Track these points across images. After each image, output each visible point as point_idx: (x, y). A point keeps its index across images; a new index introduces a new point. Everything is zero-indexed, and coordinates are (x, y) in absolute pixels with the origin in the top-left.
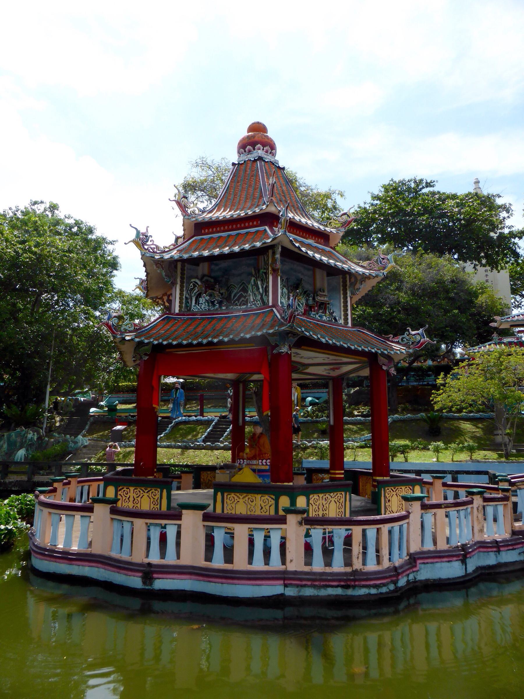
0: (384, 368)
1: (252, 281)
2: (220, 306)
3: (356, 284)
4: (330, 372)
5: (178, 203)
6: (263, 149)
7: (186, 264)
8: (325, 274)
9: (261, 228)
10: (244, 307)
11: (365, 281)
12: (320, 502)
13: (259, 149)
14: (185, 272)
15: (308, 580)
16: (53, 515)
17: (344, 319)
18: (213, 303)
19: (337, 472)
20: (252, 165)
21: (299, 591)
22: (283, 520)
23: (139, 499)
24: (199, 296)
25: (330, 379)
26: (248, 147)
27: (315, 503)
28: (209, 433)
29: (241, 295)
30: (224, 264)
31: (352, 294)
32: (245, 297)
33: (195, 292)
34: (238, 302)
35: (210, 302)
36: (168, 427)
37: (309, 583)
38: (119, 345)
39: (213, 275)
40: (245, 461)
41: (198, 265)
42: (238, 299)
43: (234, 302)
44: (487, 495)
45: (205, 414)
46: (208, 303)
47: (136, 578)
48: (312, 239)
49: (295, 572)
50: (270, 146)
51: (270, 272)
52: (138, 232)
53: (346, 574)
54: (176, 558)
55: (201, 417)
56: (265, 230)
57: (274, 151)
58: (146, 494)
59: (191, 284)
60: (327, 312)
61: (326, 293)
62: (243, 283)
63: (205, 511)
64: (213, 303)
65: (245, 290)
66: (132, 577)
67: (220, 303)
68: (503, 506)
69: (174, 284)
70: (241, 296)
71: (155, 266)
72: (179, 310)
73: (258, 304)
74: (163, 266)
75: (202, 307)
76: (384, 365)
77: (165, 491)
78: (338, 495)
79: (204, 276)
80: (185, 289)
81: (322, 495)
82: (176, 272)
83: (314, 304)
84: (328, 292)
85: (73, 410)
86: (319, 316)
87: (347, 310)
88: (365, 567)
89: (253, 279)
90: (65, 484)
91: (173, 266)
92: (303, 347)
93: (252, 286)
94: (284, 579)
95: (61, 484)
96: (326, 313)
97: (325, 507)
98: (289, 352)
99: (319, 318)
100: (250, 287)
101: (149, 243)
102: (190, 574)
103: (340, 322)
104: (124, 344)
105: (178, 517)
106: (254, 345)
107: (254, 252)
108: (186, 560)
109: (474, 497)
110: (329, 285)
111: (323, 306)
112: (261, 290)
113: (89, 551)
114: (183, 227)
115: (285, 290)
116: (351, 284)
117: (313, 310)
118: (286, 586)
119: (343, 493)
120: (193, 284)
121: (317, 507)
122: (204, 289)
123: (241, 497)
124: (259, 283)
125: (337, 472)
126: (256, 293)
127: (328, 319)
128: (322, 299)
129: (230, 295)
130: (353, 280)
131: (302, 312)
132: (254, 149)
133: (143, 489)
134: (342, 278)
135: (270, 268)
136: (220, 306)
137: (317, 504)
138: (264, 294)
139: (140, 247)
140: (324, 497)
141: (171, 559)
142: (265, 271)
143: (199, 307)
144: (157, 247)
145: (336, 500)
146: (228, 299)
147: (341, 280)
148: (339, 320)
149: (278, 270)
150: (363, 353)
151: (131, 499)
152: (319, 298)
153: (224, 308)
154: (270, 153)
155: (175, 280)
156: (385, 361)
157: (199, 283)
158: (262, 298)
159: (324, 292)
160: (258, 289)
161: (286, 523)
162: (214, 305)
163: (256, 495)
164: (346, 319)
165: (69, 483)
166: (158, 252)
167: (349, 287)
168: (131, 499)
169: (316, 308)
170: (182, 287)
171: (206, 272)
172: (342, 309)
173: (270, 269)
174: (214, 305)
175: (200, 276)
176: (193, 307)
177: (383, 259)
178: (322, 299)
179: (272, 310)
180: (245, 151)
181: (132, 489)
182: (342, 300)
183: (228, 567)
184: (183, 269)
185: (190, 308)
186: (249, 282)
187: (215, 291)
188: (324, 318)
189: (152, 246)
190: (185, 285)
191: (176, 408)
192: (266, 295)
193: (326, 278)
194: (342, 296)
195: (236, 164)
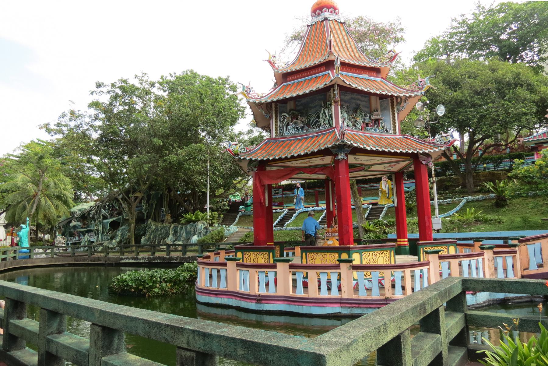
0: (424, 162)
1: (322, 111)
2: (302, 130)
3: (401, 103)
4: (390, 168)
5: (270, 62)
6: (328, 11)
8: (378, 98)
9: (326, 72)
10: (317, 129)
11: (408, 100)
12: (371, 257)
13: (325, 11)
15: (356, 304)
16: (205, 269)
17: (393, 130)
19: (402, 240)
20: (321, 24)
21: (351, 311)
22: (338, 267)
23: (256, 259)
24: (288, 124)
25: (393, 173)
26: (318, 11)
29: (317, 121)
30: (304, 101)
32: (319, 122)
36: (293, 216)
37: (357, 306)
38: (237, 162)
39: (298, 108)
41: (287, 103)
42: (315, 124)
44: (496, 250)
45: (320, 205)
46: (294, 129)
47: (252, 304)
48: (366, 74)
49: (348, 299)
50: (332, 8)
52: (244, 87)
53: (381, 300)
54: (275, 291)
55: (317, 208)
56: (329, 73)
57: (337, 11)
58: (260, 256)
59: (282, 117)
60: (380, 126)
61: (379, 112)
63: (291, 263)
64: (297, 128)
65: (319, 117)
66: (250, 303)
67: (302, 128)
68: (511, 258)
69: (271, 118)
70: (317, 121)
71: (257, 107)
75: (291, 132)
77: (271, 253)
78: (385, 252)
79: (291, 110)
80: (278, 121)
81: (372, 252)
82: (272, 110)
83: (370, 121)
84: (381, 111)
85: (228, 208)
86: (374, 130)
87: (395, 123)
88: (394, 296)
89: (323, 109)
90: (215, 254)
91: (269, 106)
92: (357, 154)
93: (323, 114)
94: (341, 303)
95: (213, 253)
96: (379, 127)
97: (375, 260)
98: (346, 158)
100: (321, 115)
101: (251, 92)
102: (284, 300)
104: (241, 162)
105: (274, 267)
107: (319, 92)
108: (281, 292)
109: (485, 251)
110: (381, 106)
111: (376, 122)
112: (328, 117)
113: (226, 290)
115: (345, 115)
116: (397, 103)
118: (341, 307)
119: (388, 251)
121: (368, 260)
122: (291, 119)
123: (318, 255)
124: (326, 111)
125: (402, 240)
126: (326, 119)
128: (376, 117)
129: (309, 122)
130: (399, 100)
132: (322, 12)
133: (258, 253)
134: (391, 100)
136: (302, 130)
139: (246, 96)
140: (374, 254)
141: (272, 292)
144: (257, 95)
145: (383, 256)
146: (308, 125)
147: (390, 101)
148: (390, 131)
149: (338, 101)
150: (407, 154)
151: (252, 259)
152: (374, 117)
153: (305, 131)
154: (334, 13)
155: (272, 115)
156: (424, 157)
157: (287, 116)
158: (329, 122)
159: (377, 111)
160: (326, 116)
162: (298, 130)
163: (326, 254)
164: (395, 130)
165: (219, 254)
167: (396, 106)
168: (252, 259)
169: (372, 124)
170: (276, 119)
171: (293, 107)
172: (392, 122)
173: (332, 102)
174: (298, 130)
175: (288, 112)
177: (421, 82)
178: (376, 117)
179: (334, 131)
180: (316, 15)
181: (252, 253)
182: (391, 116)
183: (306, 296)
184: (276, 108)
186: (321, 111)
188: (378, 131)
189: (254, 94)
190: (278, 118)
191: (298, 202)
193: (379, 101)
194: (391, 113)
195: (309, 26)
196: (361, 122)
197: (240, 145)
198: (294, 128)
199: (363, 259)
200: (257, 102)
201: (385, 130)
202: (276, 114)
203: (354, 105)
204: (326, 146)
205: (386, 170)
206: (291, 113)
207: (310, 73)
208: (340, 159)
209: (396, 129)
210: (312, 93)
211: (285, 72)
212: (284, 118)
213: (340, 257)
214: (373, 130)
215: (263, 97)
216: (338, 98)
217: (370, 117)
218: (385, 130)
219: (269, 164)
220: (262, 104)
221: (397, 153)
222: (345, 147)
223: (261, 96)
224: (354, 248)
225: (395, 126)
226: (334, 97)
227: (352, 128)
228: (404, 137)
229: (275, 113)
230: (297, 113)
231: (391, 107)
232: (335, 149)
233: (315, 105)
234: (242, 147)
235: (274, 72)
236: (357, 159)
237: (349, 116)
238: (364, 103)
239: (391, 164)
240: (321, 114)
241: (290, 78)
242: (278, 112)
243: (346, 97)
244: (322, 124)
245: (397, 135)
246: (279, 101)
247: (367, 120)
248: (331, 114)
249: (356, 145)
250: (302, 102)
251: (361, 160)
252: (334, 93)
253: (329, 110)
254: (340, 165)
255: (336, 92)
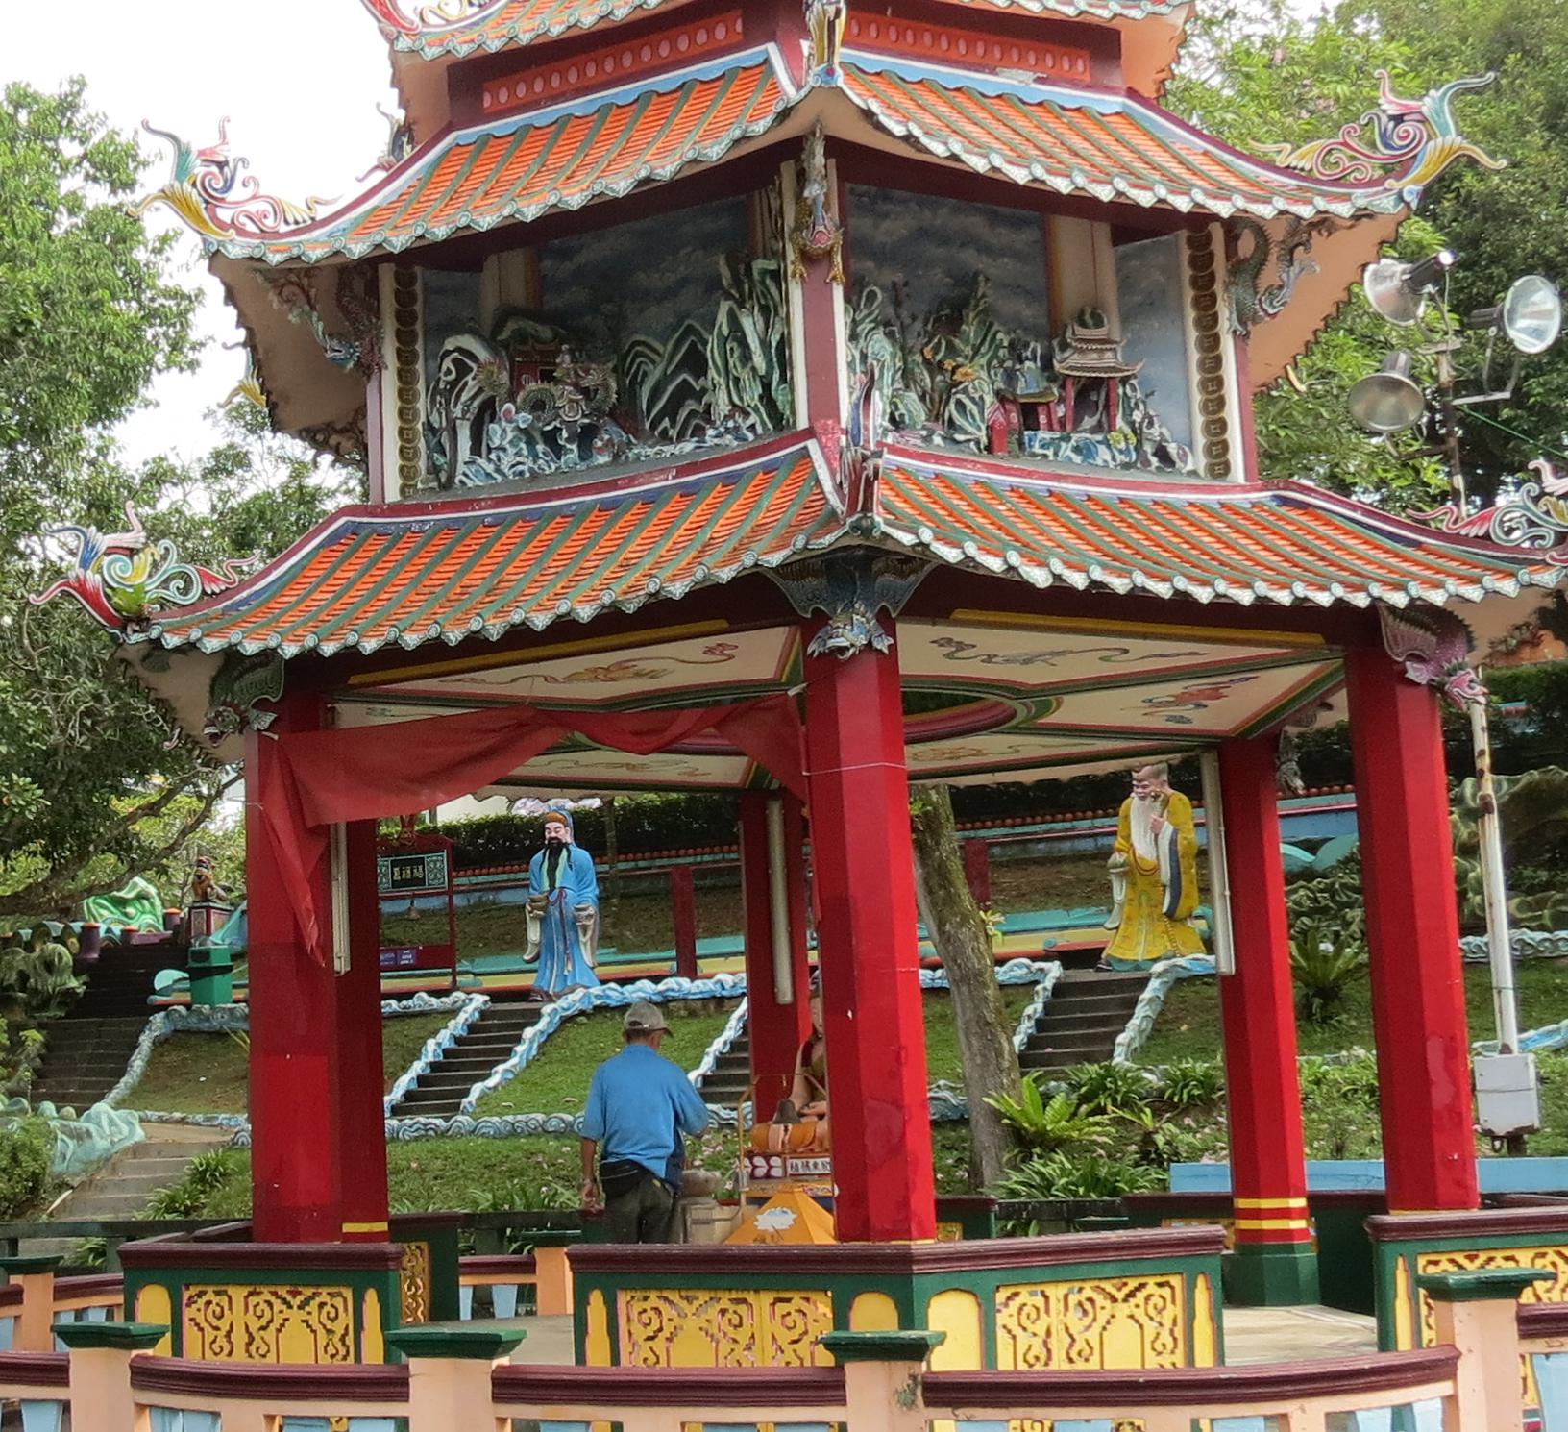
1: (722, 318)
2: (586, 453)
4: (1187, 711)
7: (418, 270)
10: (688, 446)
12: (1054, 1319)
14: (418, 307)
17: (1208, 450)
18: (551, 438)
24: (487, 412)
27: (1026, 1323)
28: (721, 1061)
30: (594, 250)
31: (1242, 321)
33: (464, 397)
34: (673, 423)
35: (537, 436)
38: (140, 671)
39: (553, 302)
40: (776, 1161)
41: (475, 265)
42: (671, 410)
43: (653, 427)
46: (531, 443)
51: (790, 268)
52: (183, 153)
59: (447, 364)
60: (1120, 422)
61: (1112, 327)
62: (690, 330)
64: (551, 438)
65: (696, 363)
67: (585, 437)
69: (368, 368)
70: (685, 392)
71: (272, 296)
72: (402, 490)
73: (752, 428)
74: (313, 292)
75: (505, 467)
76: (1419, 659)
79: (506, 314)
80: (421, 386)
81: (1063, 1289)
82: (378, 315)
83: (1047, 391)
84: (1126, 319)
86: (1077, 450)
87: (1221, 403)
89: (725, 306)
91: (359, 286)
92: (959, 614)
93: (723, 341)
96: (1111, 428)
98: (882, 644)
99: (1077, 459)
100: (712, 350)
101: (237, 193)
103: (1190, 467)
106: (724, 624)
110: (1125, 285)
112: (759, 361)
114: (395, 92)
115: (880, 346)
117: (1043, 419)
120: (455, 361)
121: (1037, 1343)
122: (505, 377)
126: (745, 375)
127: (1120, 458)
128: (1091, 360)
129: (629, 393)
131: (978, 443)
135: (789, 248)
136: (586, 453)
137: (1040, 1328)
138: (776, 376)
140: (1073, 1299)
142: (772, 266)
143: (490, 468)
144: (278, 209)
146: (625, 414)
148: (1184, 458)
149: (829, 254)
152: (1075, 359)
155: (375, 347)
158: (767, 398)
159: (1099, 323)
160: (746, 357)
161: (842, 1401)
162: (558, 451)
164: (1218, 451)
166: (283, 228)
169: (1060, 411)
170: (406, 377)
171: (518, 293)
172: (1197, 398)
173: (791, 256)
174: (558, 451)
176: (461, 468)
178: (1091, 360)
179: (805, 454)
184: (404, 298)
185: (451, 477)
186: (710, 323)
187: (557, 381)
188: (1104, 454)
189: (253, 207)
190: (419, 367)
192: (783, 379)
193: (1107, 254)
194: (1193, 335)
196: (989, 399)
197: (158, 550)
198: (527, 435)
199: (1002, 1337)
200: (275, 259)
201: (1148, 448)
202: (405, 338)
203: (937, 280)
204: (748, 560)
205: (1158, 721)
206: (505, 335)
207: (636, 56)
208: (843, 650)
209: (1225, 447)
210: (650, 197)
211: (463, 51)
212: (462, 370)
213: (841, 1319)
214: (1066, 450)
215: (316, 224)
216: (827, 231)
217: (1047, 364)
218: (1148, 448)
219: (354, 680)
220: (311, 271)
221: (1236, 606)
222: (877, 566)
223: (304, 215)
224: (936, 1259)
225: (1223, 425)
226: (799, 227)
227: (927, 439)
228: (1285, 501)
229: (399, 335)
230: (546, 333)
231: (1189, 294)
232: (811, 582)
233: (671, 278)
234: (171, 565)
235: (394, 56)
236: (961, 646)
237: (906, 352)
238: (1002, 268)
239: (1193, 685)
240: (713, 342)
241: (503, 97)
242: (419, 327)
243: (886, 225)
244: (722, 407)
245: (1235, 488)
246: (422, 254)
247: (1029, 382)
248: (785, 343)
249: (951, 555)
250: (581, 259)
251: (989, 659)
252: (799, 197)
253: (765, 311)
254: (845, 691)
255: (813, 191)
